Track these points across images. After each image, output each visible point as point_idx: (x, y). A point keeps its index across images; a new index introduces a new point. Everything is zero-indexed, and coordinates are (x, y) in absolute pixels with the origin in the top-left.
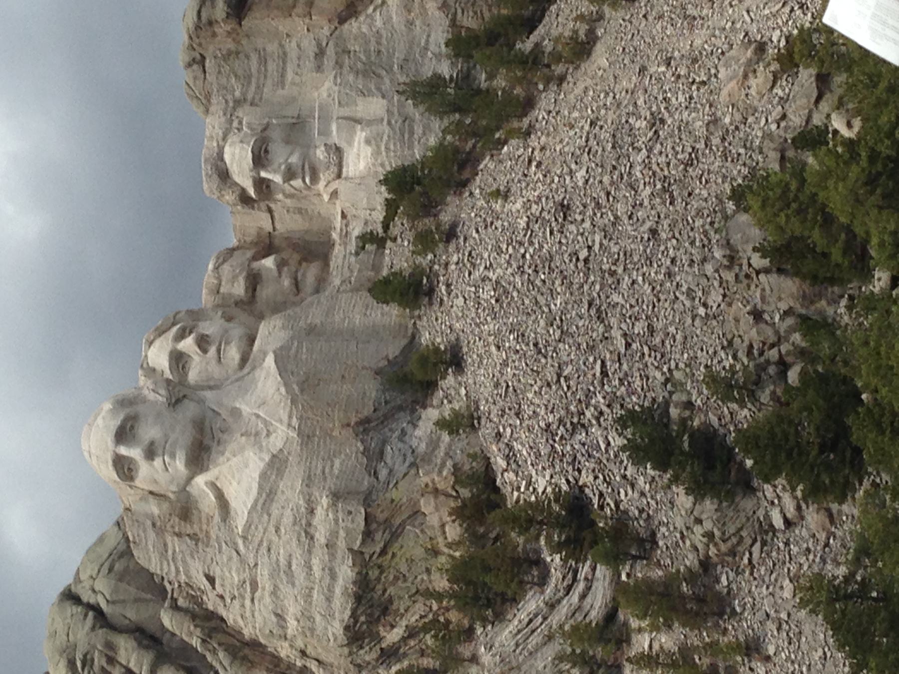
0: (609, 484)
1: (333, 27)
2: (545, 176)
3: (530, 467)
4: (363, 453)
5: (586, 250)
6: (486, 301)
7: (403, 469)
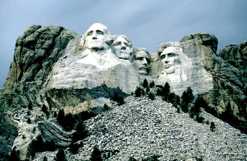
0: (90, 141)
1: (204, 66)
2: (167, 117)
4: (98, 86)
7: (94, 96)
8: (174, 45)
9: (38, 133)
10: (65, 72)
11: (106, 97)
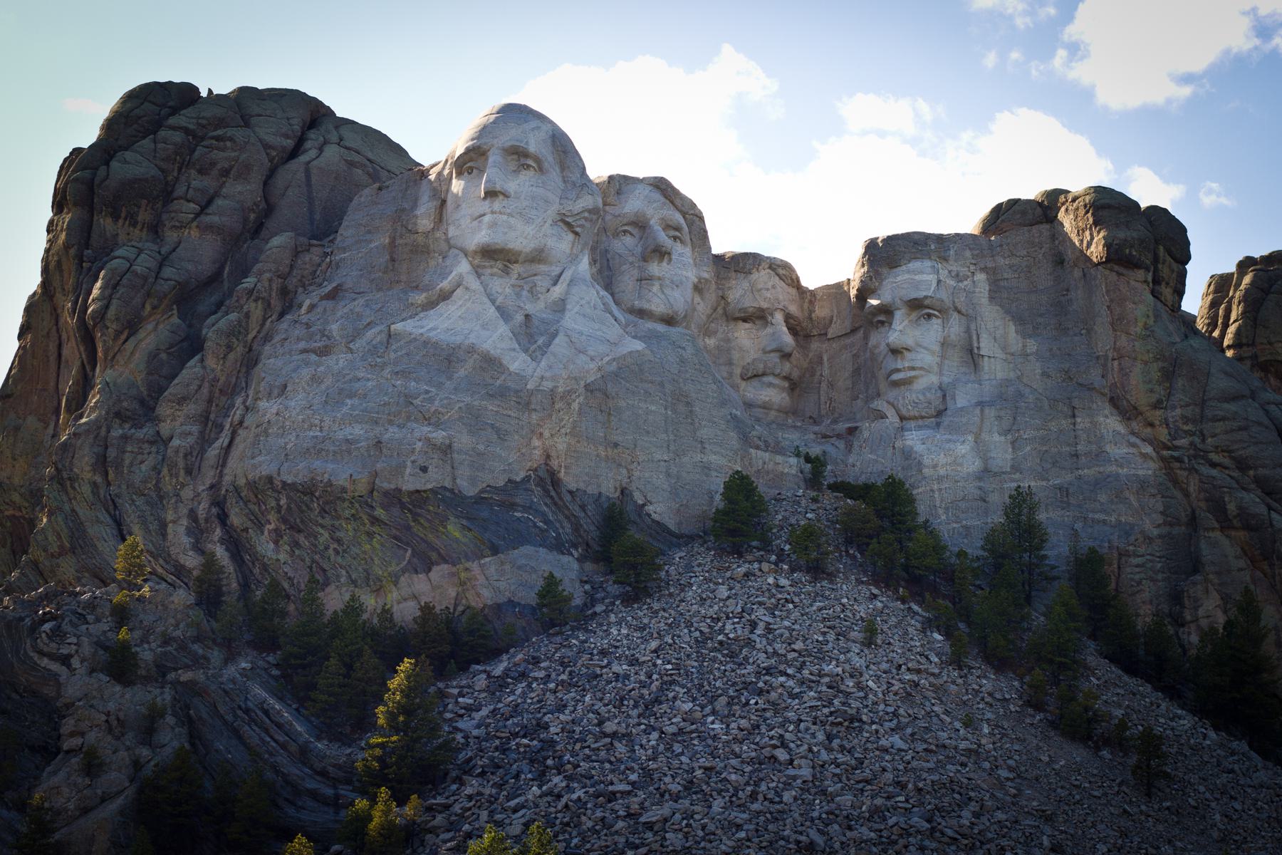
0: (461, 816)
2: (896, 694)
4: (510, 481)
5: (788, 757)
6: (721, 631)
9: (171, 738)
10: (328, 381)
11: (559, 547)
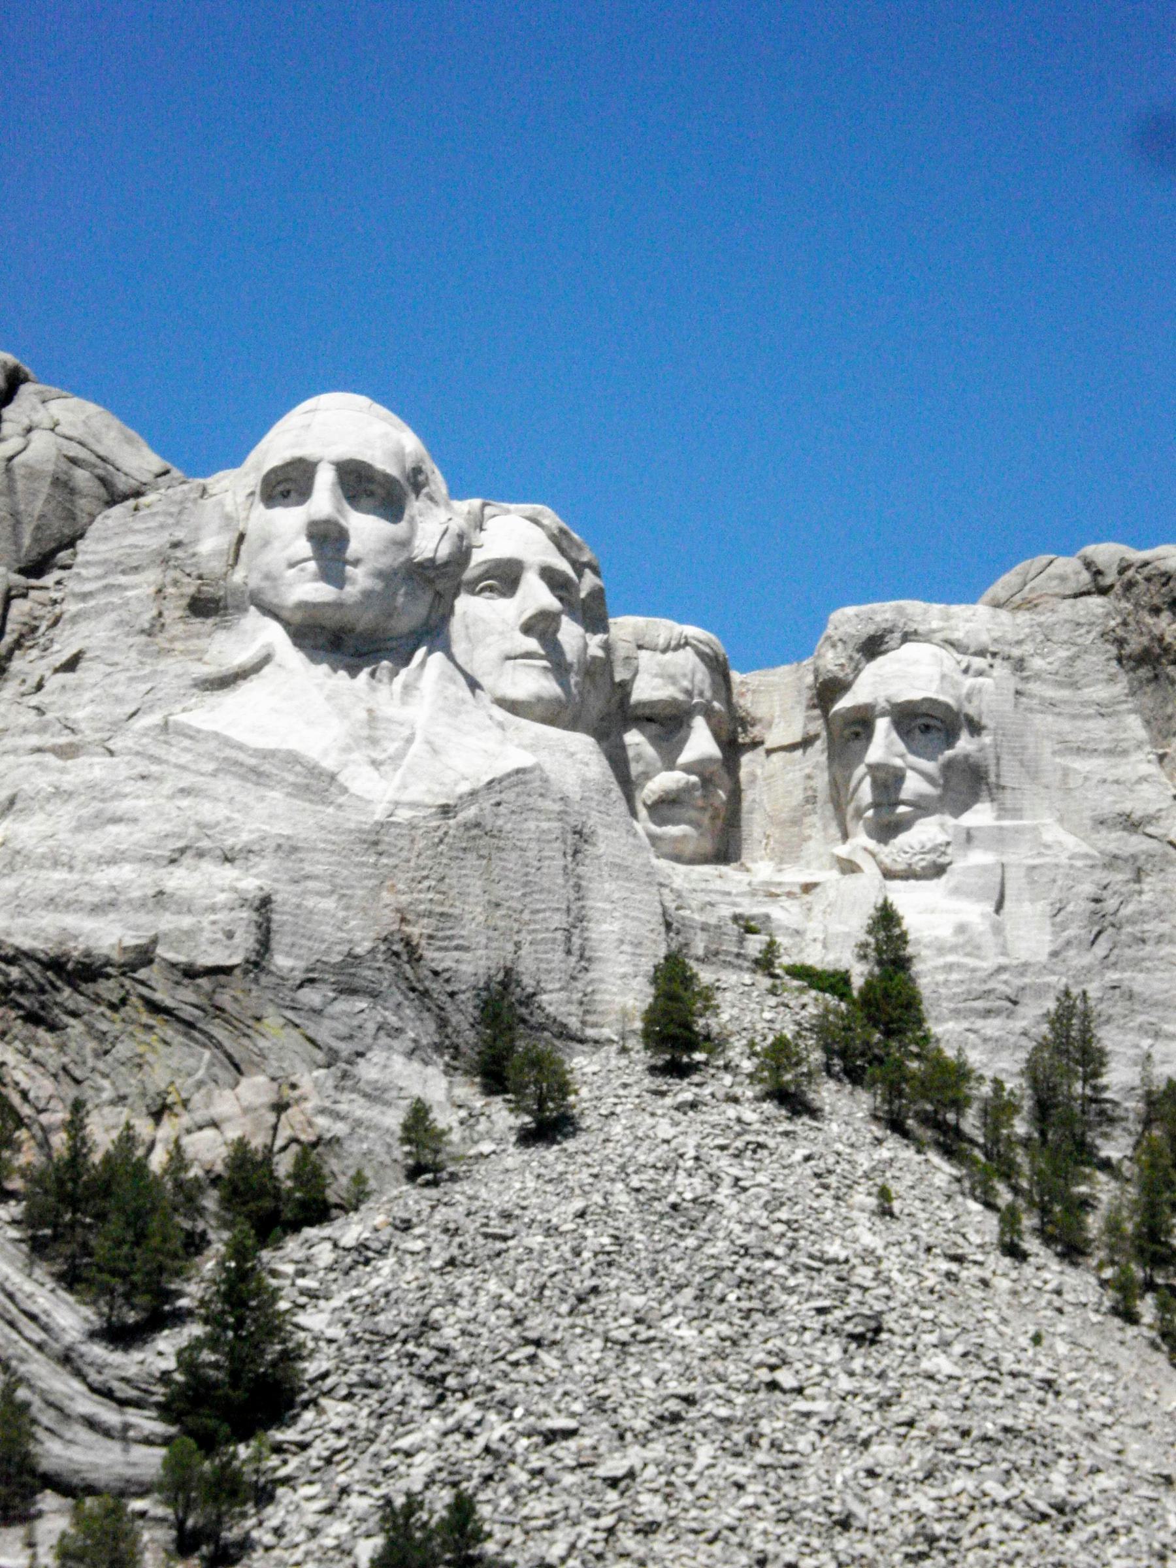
0: (329, 1461)
2: (932, 1291)
3: (346, 1295)
4: (349, 955)
6: (671, 1186)
8: (947, 634)
